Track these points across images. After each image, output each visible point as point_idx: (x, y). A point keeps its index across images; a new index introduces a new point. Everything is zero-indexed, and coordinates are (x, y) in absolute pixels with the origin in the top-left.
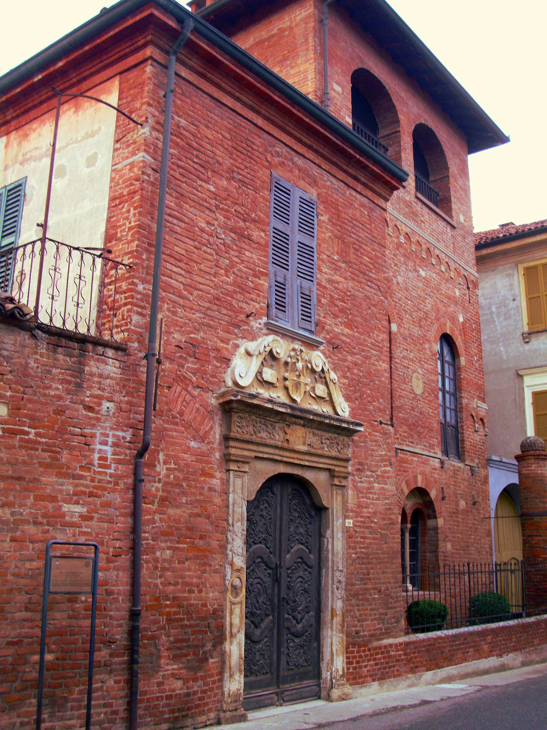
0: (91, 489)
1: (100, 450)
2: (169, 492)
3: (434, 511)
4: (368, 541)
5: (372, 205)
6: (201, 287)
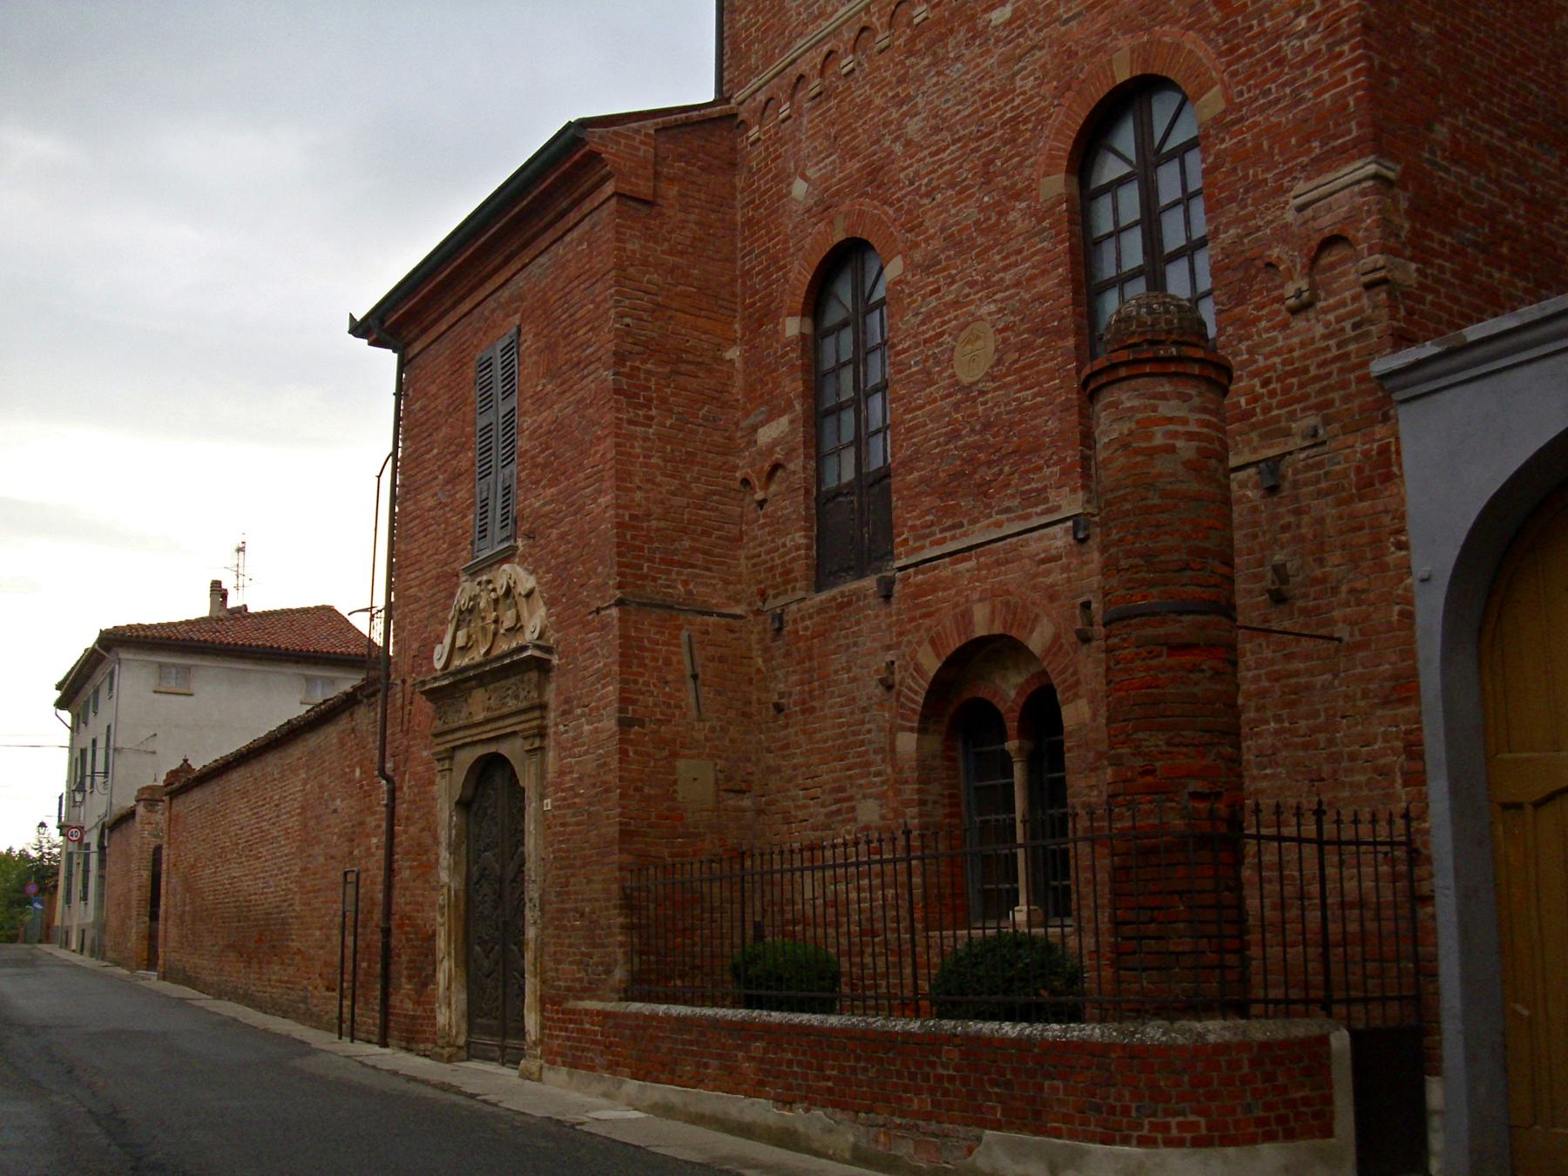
4: (569, 829)
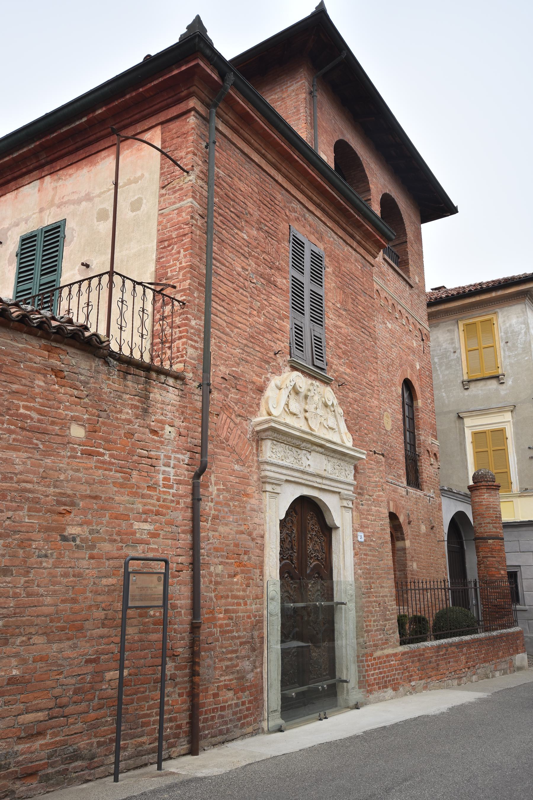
0: (157, 508)
1: (164, 471)
2: (219, 511)
3: (402, 534)
4: (369, 558)
5: (363, 261)
6: (240, 325)
